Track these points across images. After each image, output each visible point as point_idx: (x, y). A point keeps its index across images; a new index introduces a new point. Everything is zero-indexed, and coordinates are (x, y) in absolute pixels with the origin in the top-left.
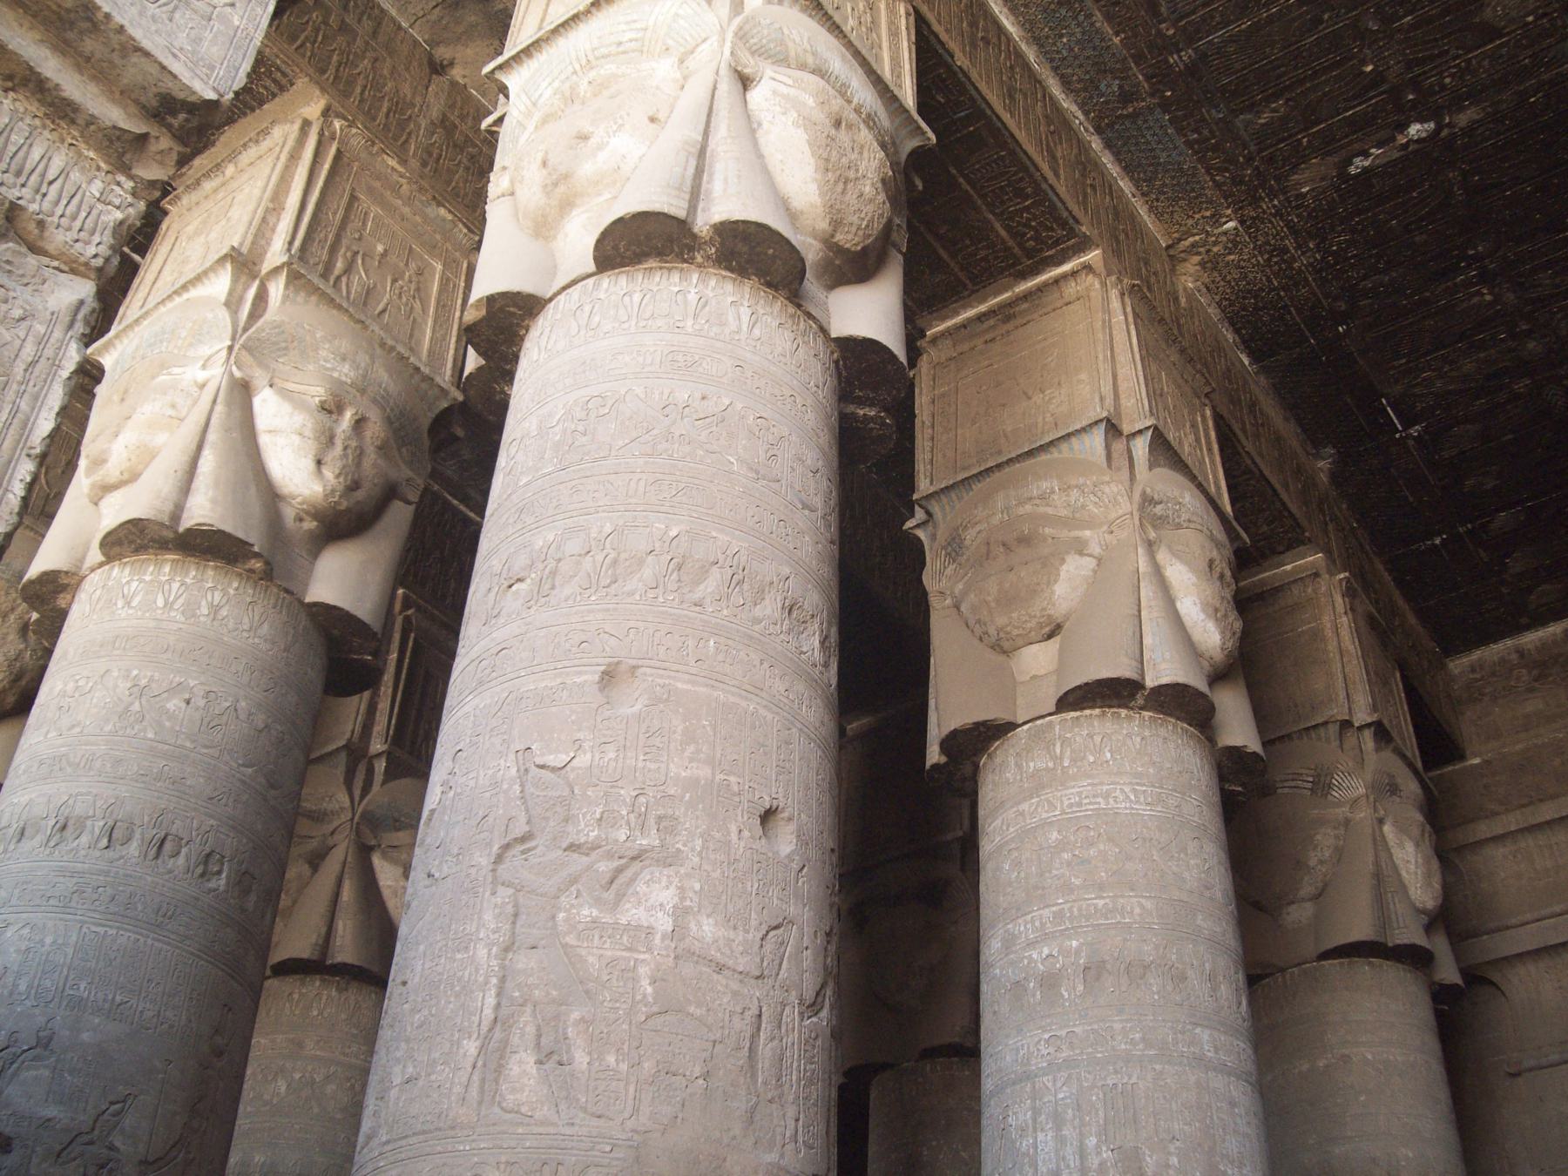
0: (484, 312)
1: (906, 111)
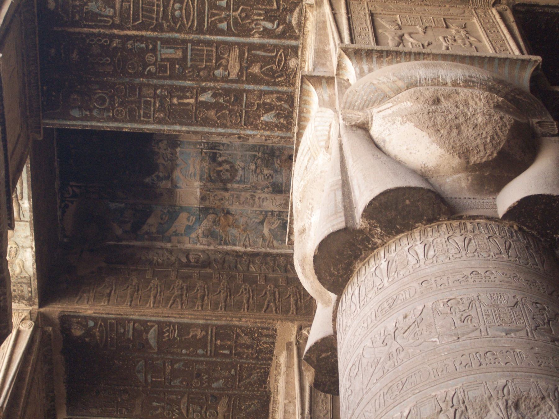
0: (313, 370)
1: (517, 60)
